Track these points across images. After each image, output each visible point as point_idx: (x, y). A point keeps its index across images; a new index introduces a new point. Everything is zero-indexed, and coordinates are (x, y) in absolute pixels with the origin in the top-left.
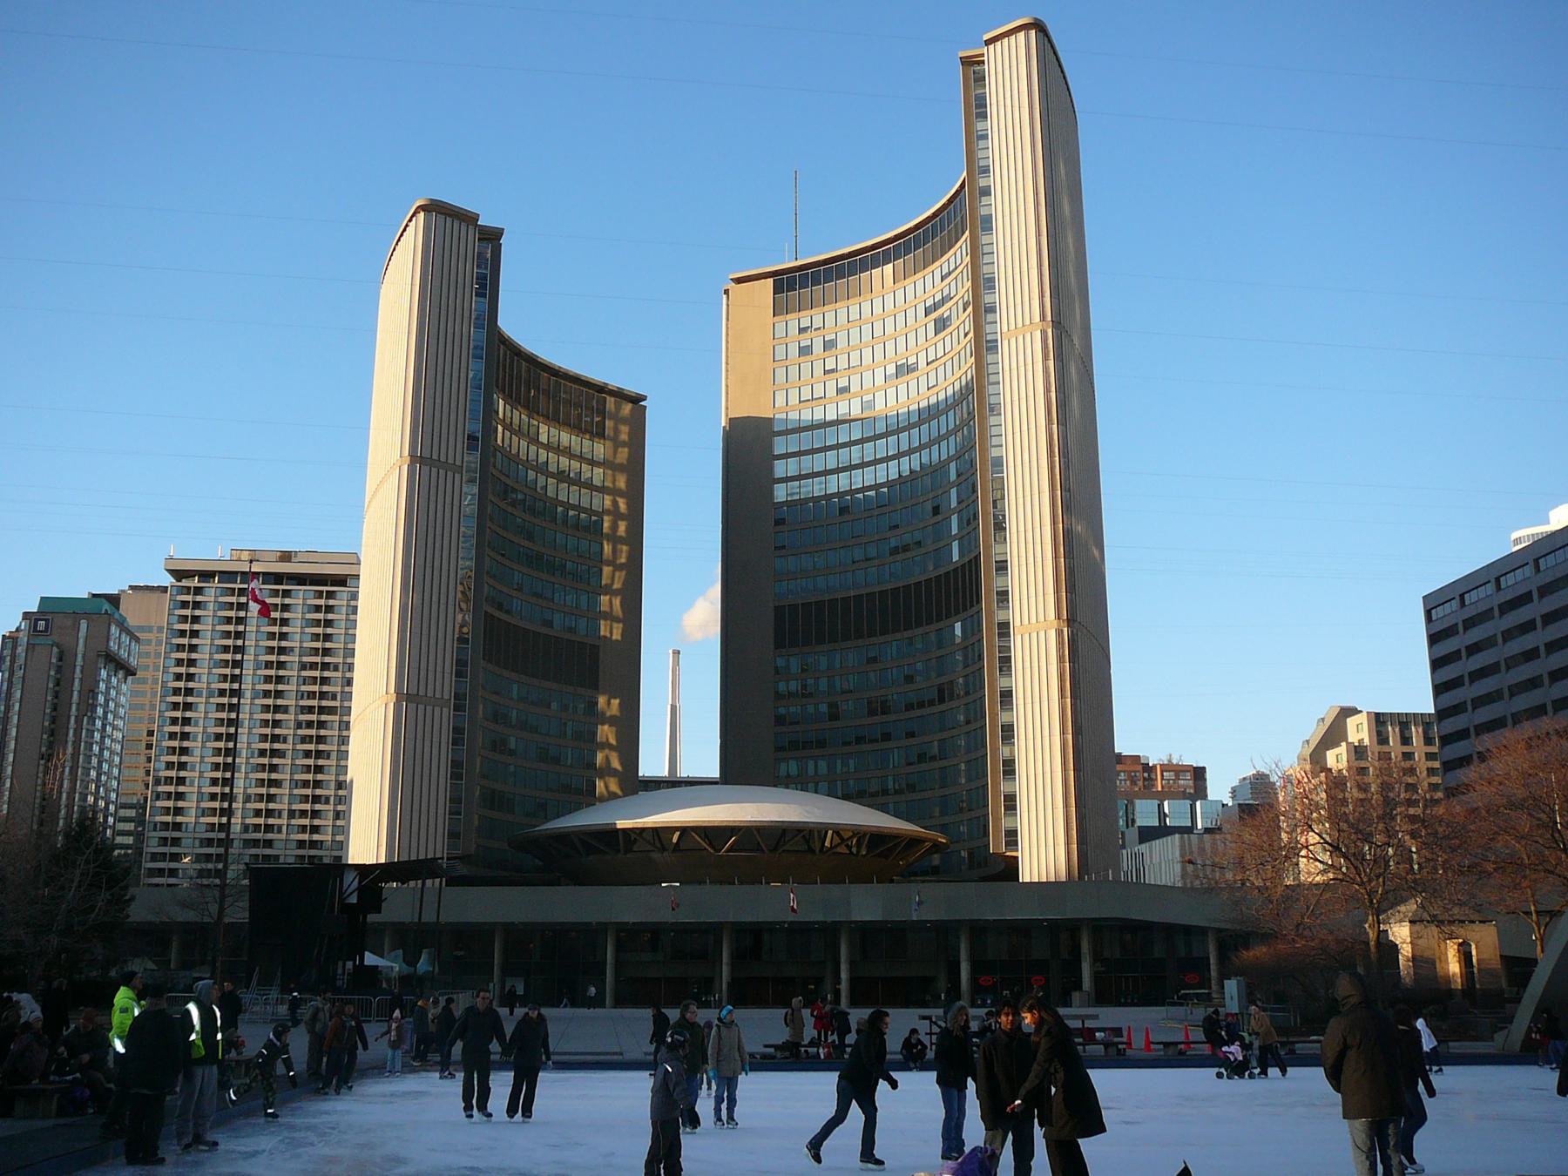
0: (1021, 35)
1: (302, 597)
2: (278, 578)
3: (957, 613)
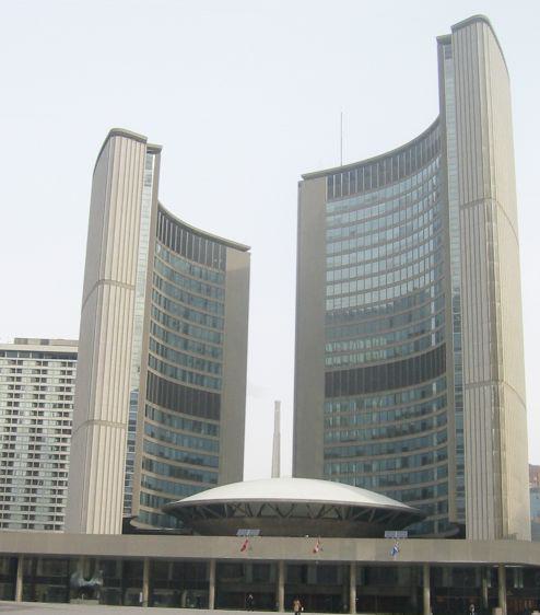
0: (473, 26)
1: (54, 367)
2: (40, 354)
3: (434, 377)
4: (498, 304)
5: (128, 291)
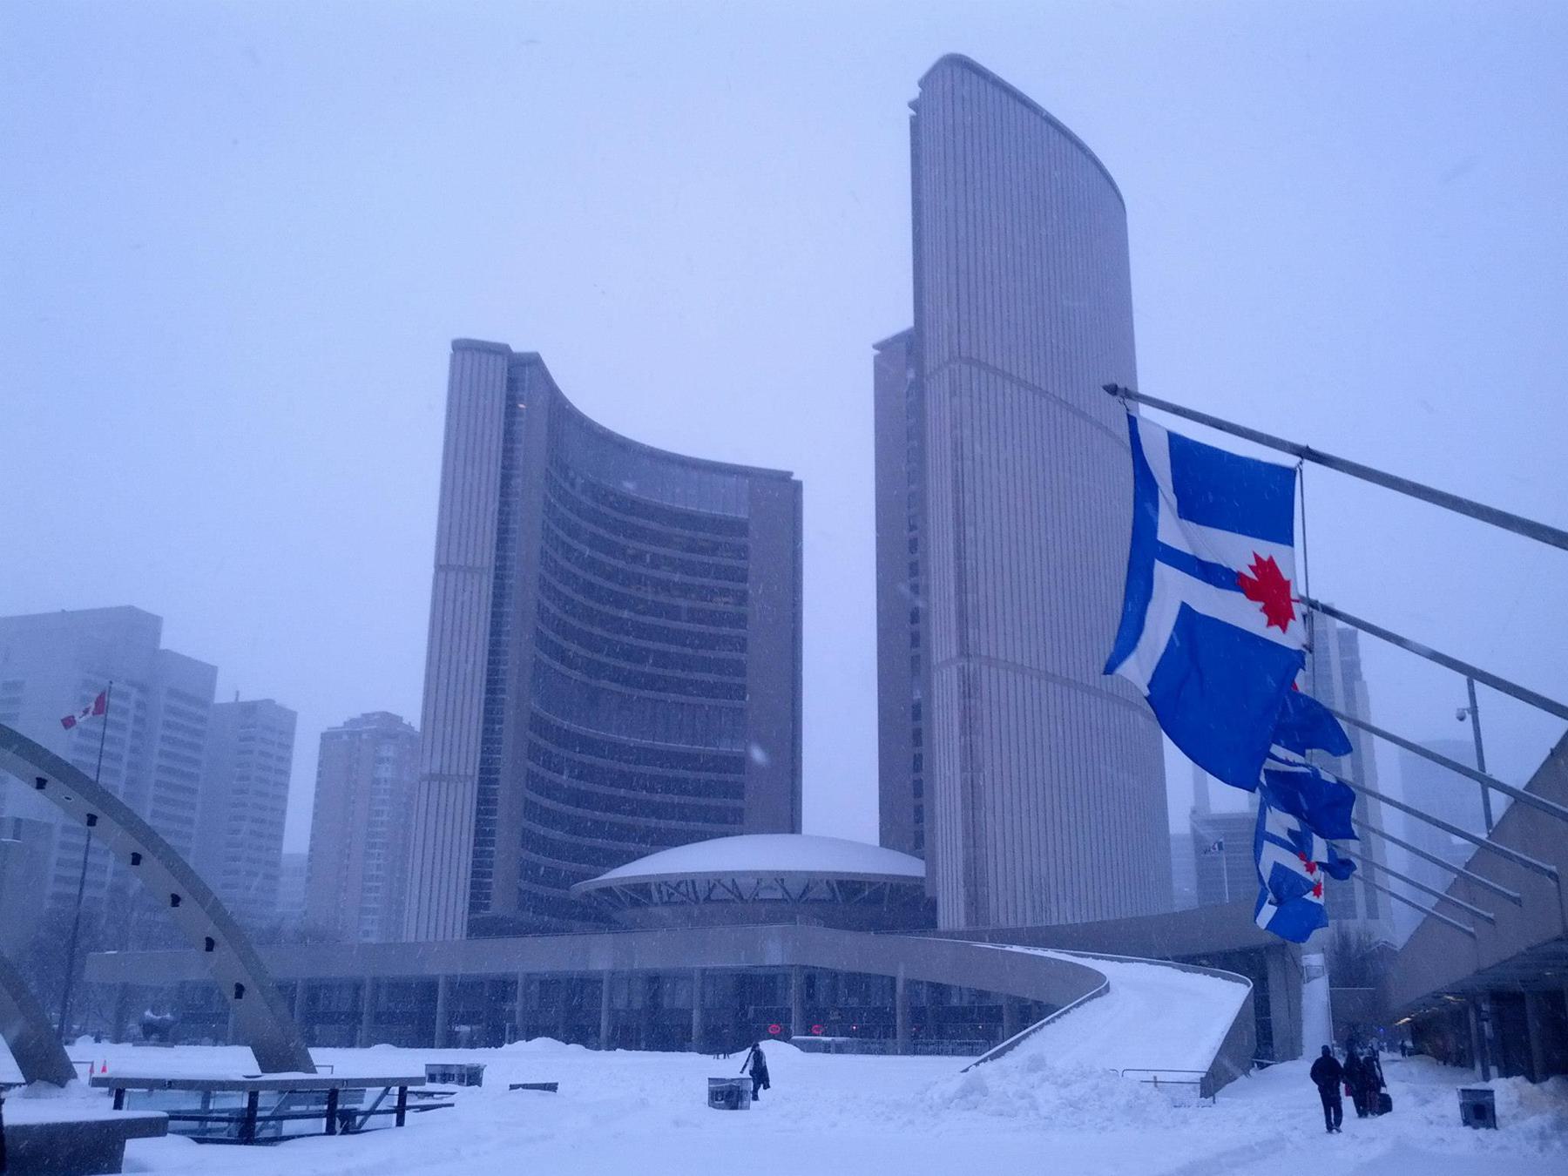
4: (970, 532)
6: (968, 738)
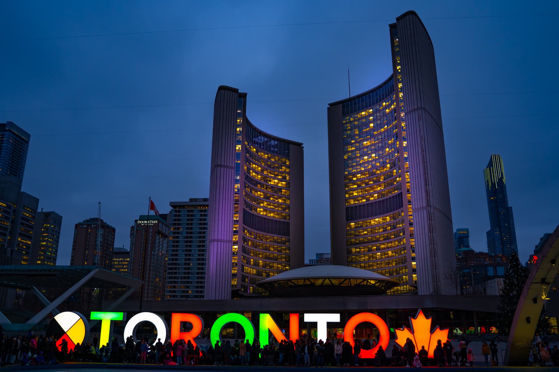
0: (407, 17)
5: (230, 170)
6: (432, 233)
